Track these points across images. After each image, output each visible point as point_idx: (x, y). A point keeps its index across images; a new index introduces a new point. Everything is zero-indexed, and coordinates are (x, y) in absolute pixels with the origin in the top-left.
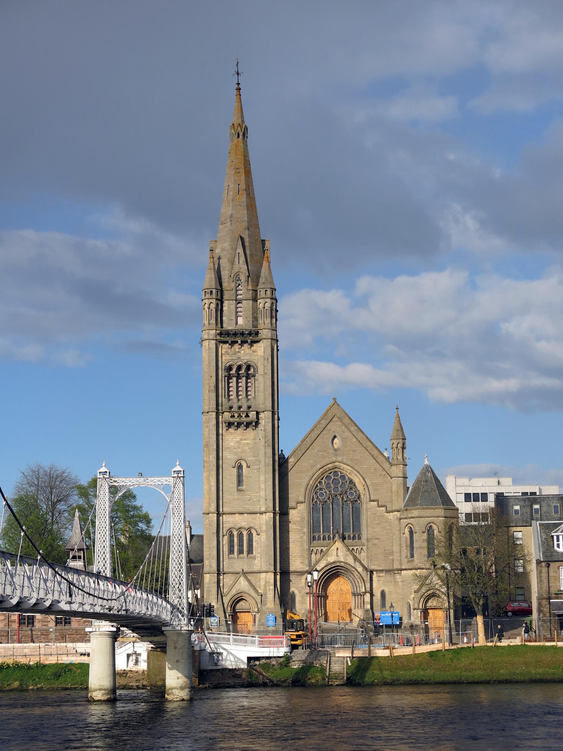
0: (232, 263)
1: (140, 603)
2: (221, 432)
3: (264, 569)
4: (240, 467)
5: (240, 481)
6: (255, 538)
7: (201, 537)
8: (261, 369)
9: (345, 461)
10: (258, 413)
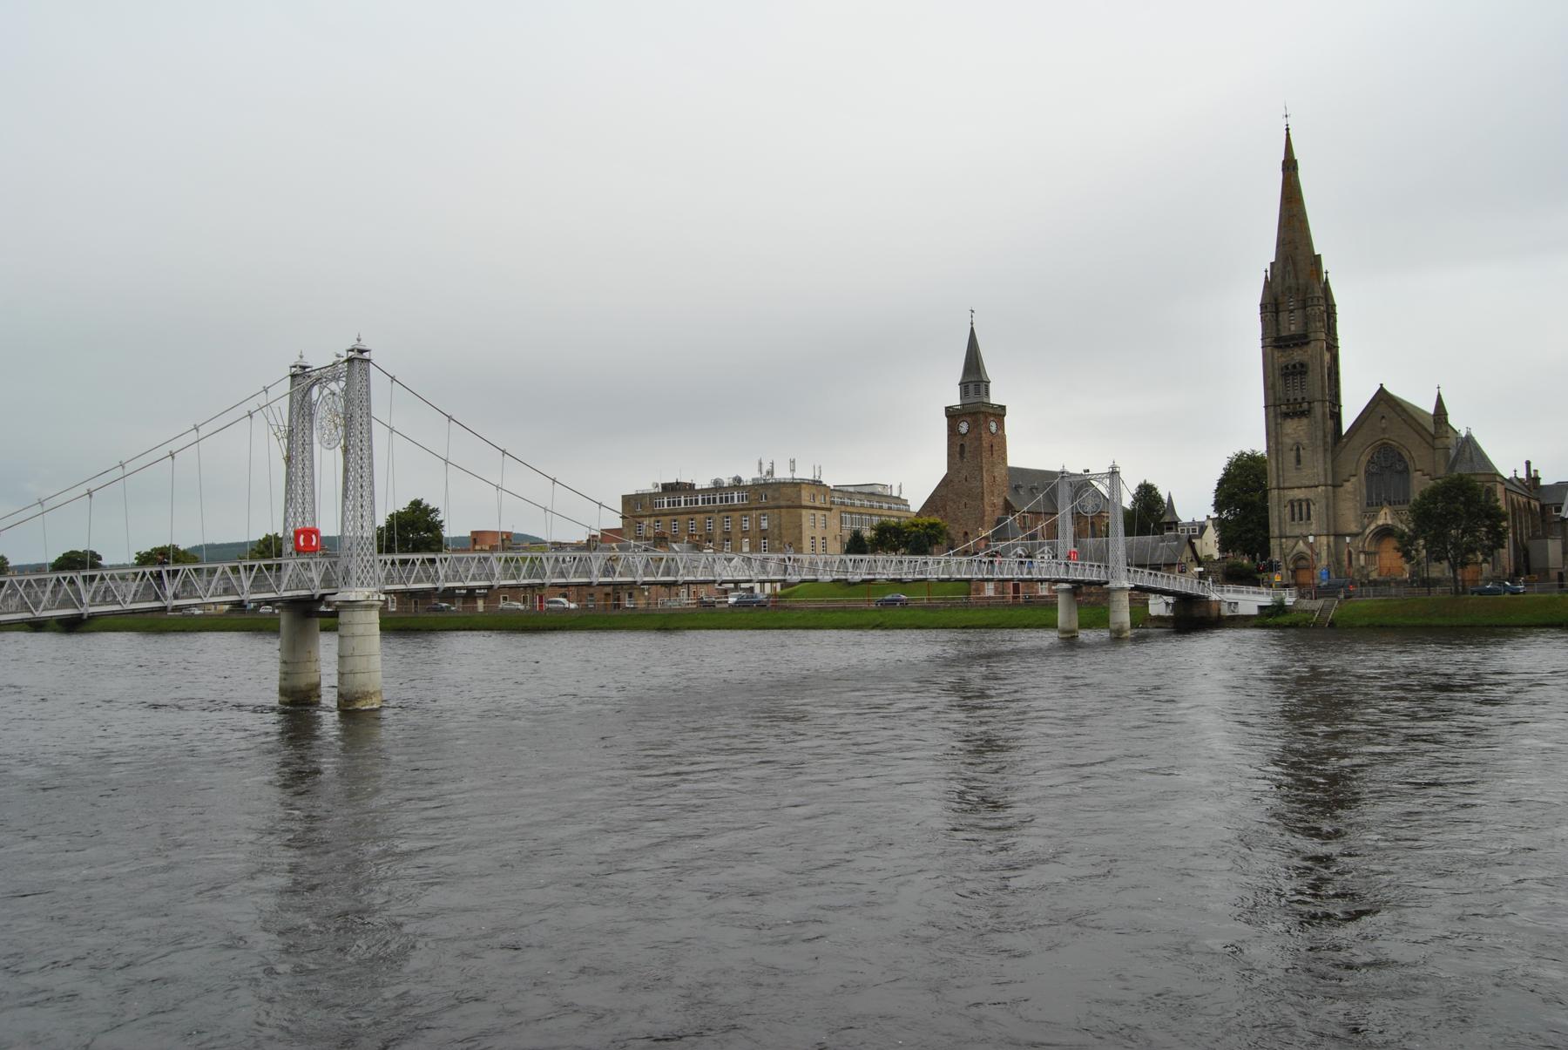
0: (1283, 278)
5: (1299, 461)
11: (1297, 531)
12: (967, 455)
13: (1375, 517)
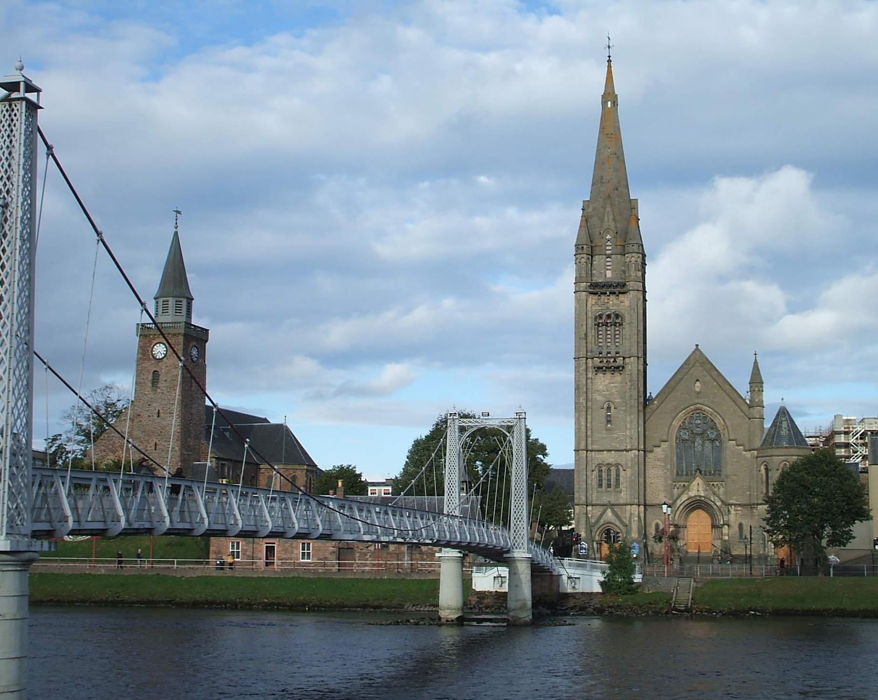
1: (489, 535)
2: (590, 375)
3: (629, 501)
4: (609, 408)
6: (622, 473)
7: (205, 553)
8: (627, 319)
9: (706, 403)
10: (624, 358)
11: (605, 499)
12: (162, 384)
13: (686, 488)
